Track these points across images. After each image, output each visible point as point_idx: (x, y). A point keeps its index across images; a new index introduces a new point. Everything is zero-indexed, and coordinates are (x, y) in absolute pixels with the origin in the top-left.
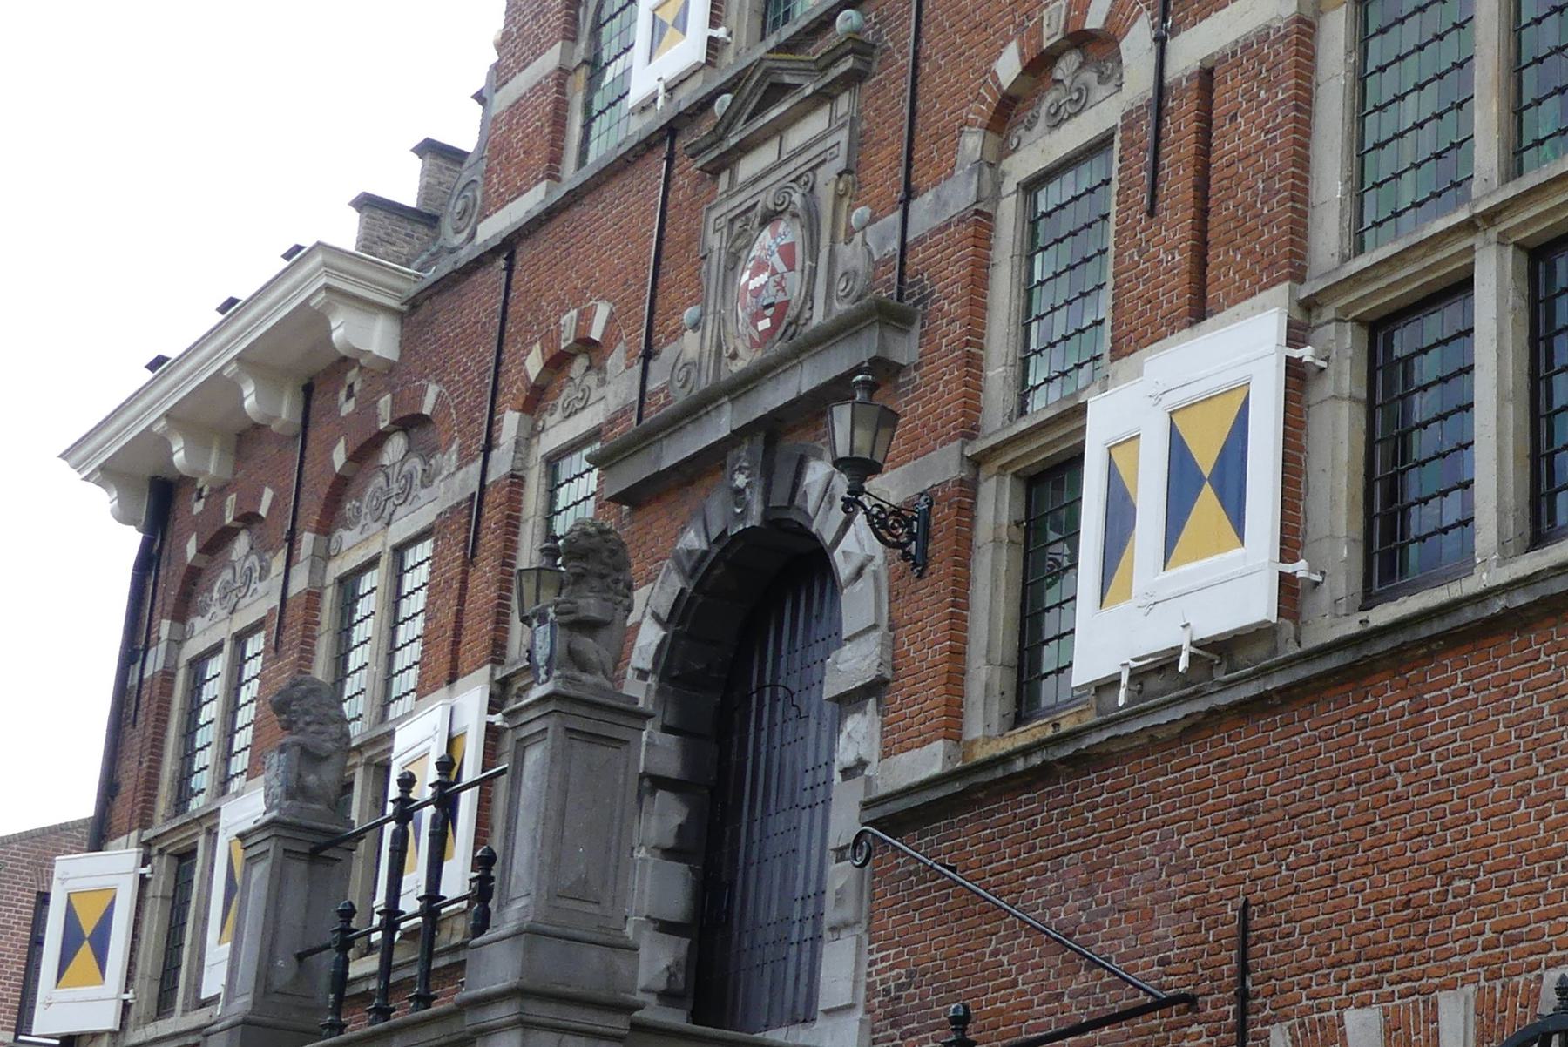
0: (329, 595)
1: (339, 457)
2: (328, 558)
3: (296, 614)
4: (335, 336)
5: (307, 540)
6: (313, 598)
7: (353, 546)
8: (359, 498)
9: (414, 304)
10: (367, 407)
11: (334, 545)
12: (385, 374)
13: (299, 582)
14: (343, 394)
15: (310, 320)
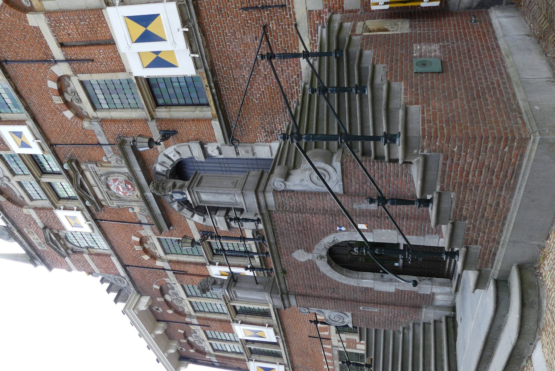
0: (198, 314)
1: (170, 312)
2: (190, 315)
3: (202, 322)
4: (144, 309)
5: (187, 320)
6: (198, 318)
7: (188, 309)
8: (178, 307)
9: (139, 292)
10: (159, 303)
11: (188, 313)
12: (153, 299)
13: (195, 321)
14: (158, 311)
15: (141, 315)
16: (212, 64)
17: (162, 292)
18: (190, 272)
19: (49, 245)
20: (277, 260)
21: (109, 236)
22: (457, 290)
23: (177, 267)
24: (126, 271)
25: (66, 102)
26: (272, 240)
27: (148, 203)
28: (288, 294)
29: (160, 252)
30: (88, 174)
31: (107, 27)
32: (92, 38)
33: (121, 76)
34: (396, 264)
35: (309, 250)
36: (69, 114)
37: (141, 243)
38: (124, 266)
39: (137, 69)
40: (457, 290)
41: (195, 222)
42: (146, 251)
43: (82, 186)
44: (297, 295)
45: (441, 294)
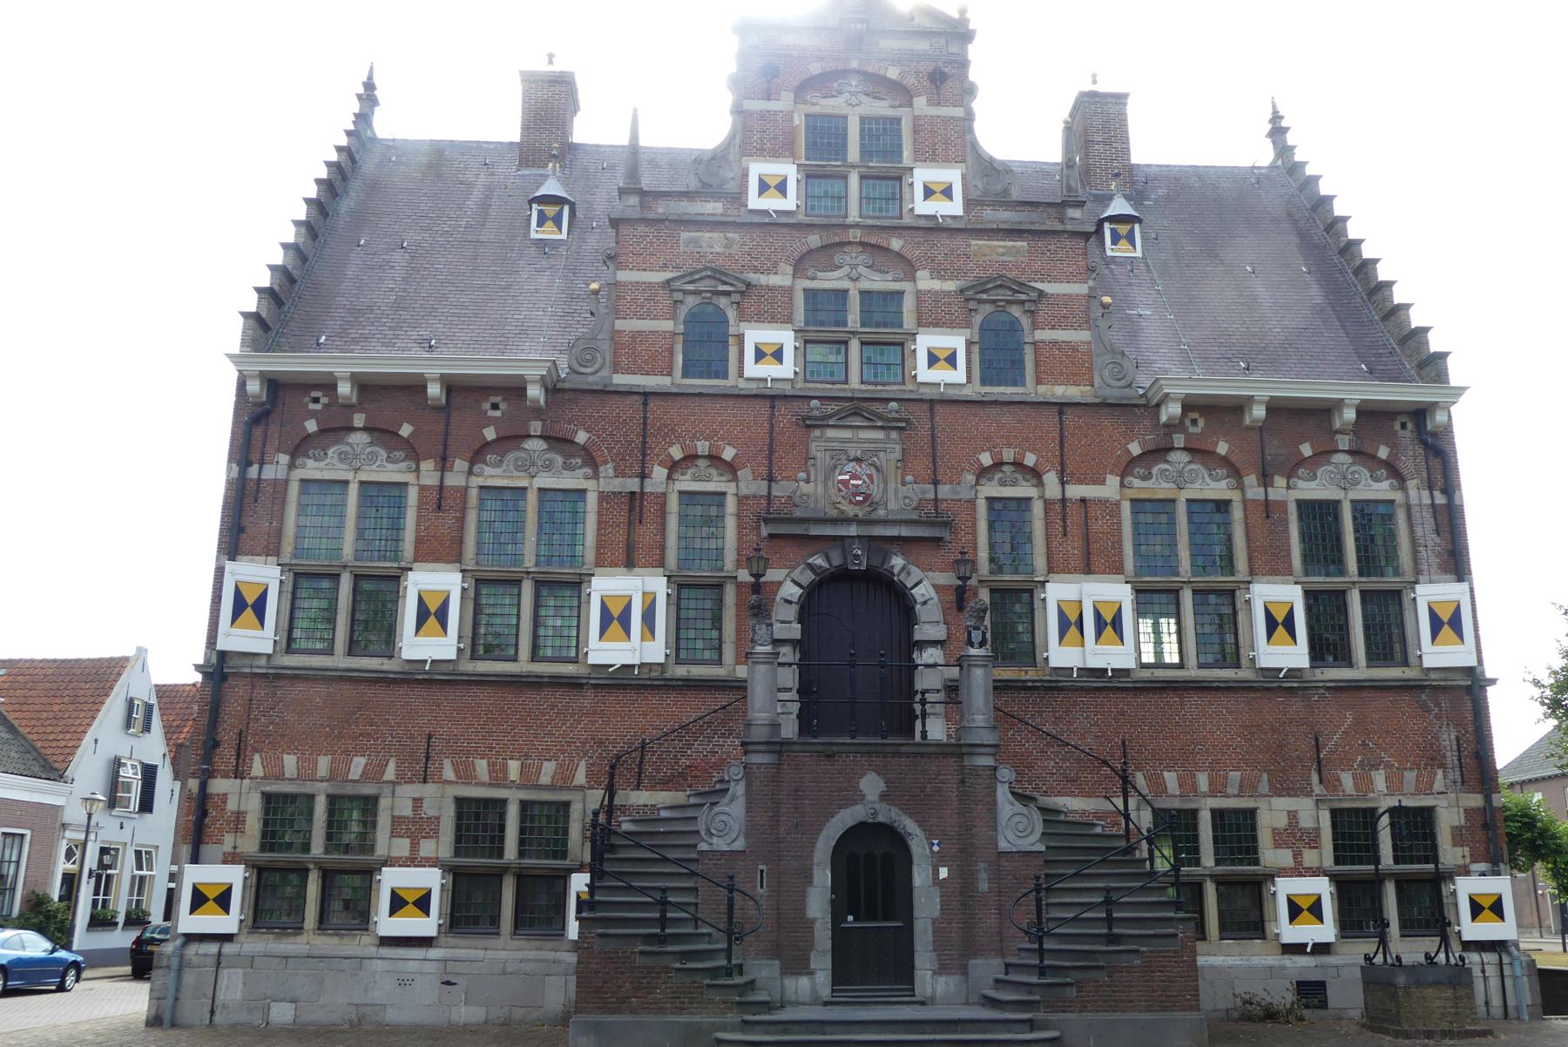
1: (490, 434)
5: (460, 465)
12: (537, 412)
16: (1062, 689)
17: (559, 441)
18: (640, 530)
19: (705, 269)
20: (864, 749)
21: (731, 402)
22: (826, 1004)
23: (650, 508)
24: (628, 393)
25: (1003, 464)
26: (904, 749)
27: (834, 521)
28: (779, 752)
29: (686, 483)
30: (879, 435)
31: (1104, 573)
32: (1095, 546)
33: (1040, 562)
34: (850, 918)
35: (884, 797)
36: (986, 459)
37: (714, 459)
38: (646, 395)
39: (1058, 592)
40: (826, 1004)
41: (780, 583)
42: (691, 458)
43: (855, 414)
44: (778, 765)
45: (814, 985)
